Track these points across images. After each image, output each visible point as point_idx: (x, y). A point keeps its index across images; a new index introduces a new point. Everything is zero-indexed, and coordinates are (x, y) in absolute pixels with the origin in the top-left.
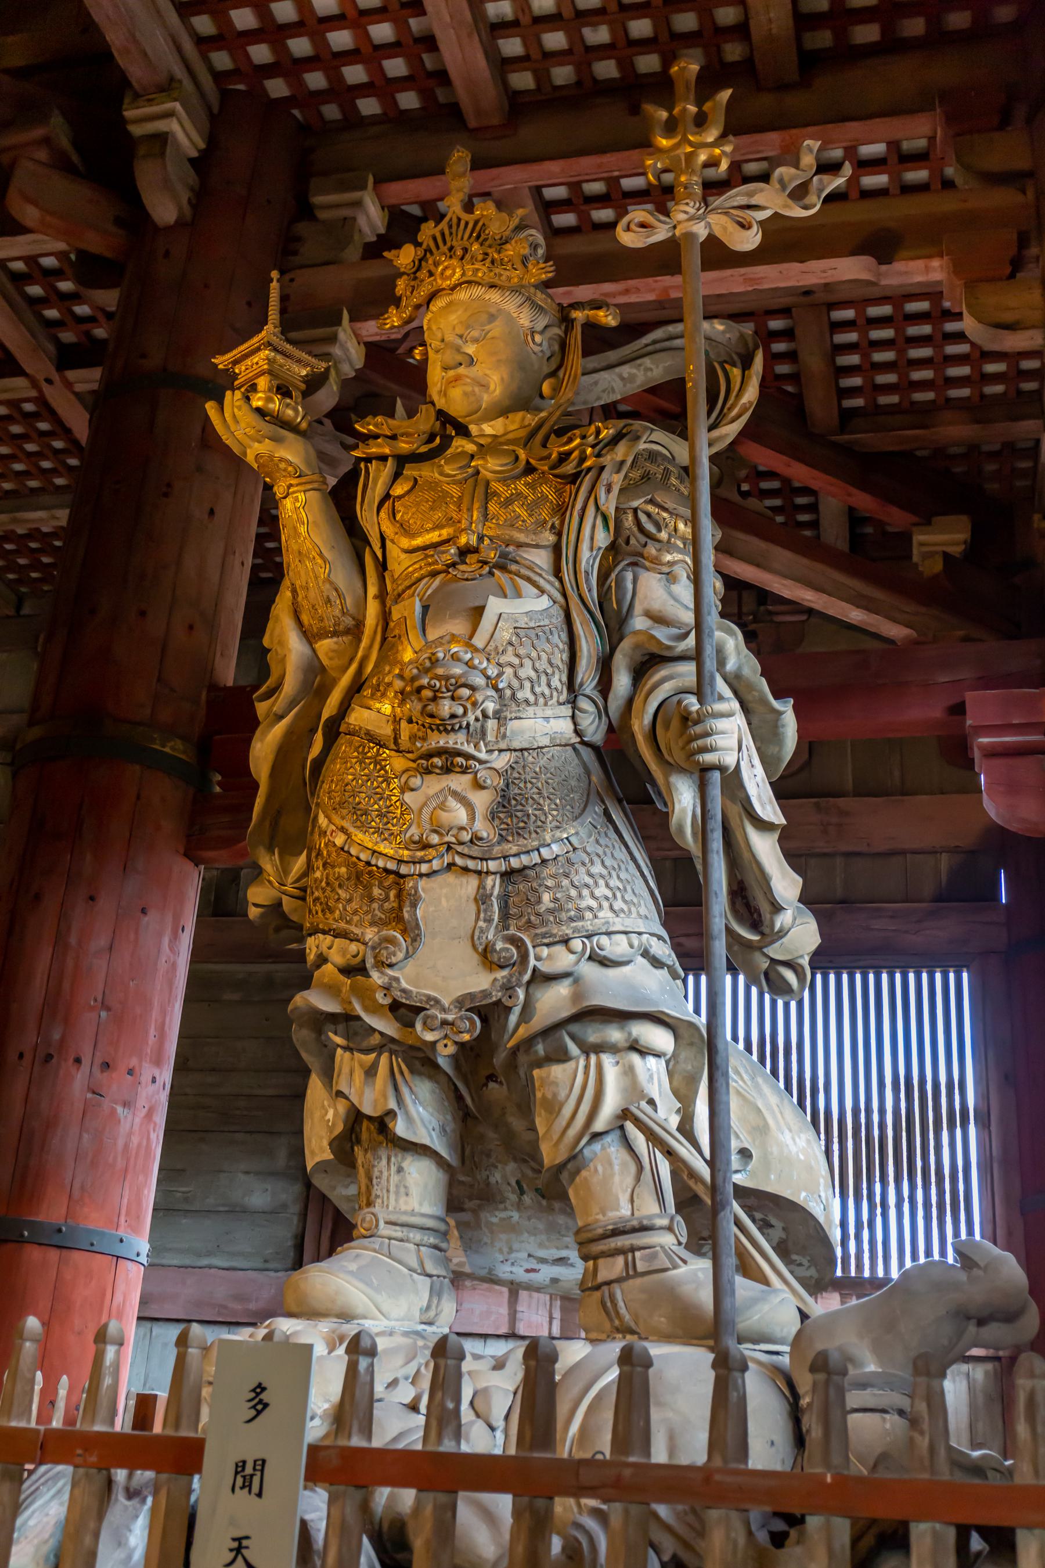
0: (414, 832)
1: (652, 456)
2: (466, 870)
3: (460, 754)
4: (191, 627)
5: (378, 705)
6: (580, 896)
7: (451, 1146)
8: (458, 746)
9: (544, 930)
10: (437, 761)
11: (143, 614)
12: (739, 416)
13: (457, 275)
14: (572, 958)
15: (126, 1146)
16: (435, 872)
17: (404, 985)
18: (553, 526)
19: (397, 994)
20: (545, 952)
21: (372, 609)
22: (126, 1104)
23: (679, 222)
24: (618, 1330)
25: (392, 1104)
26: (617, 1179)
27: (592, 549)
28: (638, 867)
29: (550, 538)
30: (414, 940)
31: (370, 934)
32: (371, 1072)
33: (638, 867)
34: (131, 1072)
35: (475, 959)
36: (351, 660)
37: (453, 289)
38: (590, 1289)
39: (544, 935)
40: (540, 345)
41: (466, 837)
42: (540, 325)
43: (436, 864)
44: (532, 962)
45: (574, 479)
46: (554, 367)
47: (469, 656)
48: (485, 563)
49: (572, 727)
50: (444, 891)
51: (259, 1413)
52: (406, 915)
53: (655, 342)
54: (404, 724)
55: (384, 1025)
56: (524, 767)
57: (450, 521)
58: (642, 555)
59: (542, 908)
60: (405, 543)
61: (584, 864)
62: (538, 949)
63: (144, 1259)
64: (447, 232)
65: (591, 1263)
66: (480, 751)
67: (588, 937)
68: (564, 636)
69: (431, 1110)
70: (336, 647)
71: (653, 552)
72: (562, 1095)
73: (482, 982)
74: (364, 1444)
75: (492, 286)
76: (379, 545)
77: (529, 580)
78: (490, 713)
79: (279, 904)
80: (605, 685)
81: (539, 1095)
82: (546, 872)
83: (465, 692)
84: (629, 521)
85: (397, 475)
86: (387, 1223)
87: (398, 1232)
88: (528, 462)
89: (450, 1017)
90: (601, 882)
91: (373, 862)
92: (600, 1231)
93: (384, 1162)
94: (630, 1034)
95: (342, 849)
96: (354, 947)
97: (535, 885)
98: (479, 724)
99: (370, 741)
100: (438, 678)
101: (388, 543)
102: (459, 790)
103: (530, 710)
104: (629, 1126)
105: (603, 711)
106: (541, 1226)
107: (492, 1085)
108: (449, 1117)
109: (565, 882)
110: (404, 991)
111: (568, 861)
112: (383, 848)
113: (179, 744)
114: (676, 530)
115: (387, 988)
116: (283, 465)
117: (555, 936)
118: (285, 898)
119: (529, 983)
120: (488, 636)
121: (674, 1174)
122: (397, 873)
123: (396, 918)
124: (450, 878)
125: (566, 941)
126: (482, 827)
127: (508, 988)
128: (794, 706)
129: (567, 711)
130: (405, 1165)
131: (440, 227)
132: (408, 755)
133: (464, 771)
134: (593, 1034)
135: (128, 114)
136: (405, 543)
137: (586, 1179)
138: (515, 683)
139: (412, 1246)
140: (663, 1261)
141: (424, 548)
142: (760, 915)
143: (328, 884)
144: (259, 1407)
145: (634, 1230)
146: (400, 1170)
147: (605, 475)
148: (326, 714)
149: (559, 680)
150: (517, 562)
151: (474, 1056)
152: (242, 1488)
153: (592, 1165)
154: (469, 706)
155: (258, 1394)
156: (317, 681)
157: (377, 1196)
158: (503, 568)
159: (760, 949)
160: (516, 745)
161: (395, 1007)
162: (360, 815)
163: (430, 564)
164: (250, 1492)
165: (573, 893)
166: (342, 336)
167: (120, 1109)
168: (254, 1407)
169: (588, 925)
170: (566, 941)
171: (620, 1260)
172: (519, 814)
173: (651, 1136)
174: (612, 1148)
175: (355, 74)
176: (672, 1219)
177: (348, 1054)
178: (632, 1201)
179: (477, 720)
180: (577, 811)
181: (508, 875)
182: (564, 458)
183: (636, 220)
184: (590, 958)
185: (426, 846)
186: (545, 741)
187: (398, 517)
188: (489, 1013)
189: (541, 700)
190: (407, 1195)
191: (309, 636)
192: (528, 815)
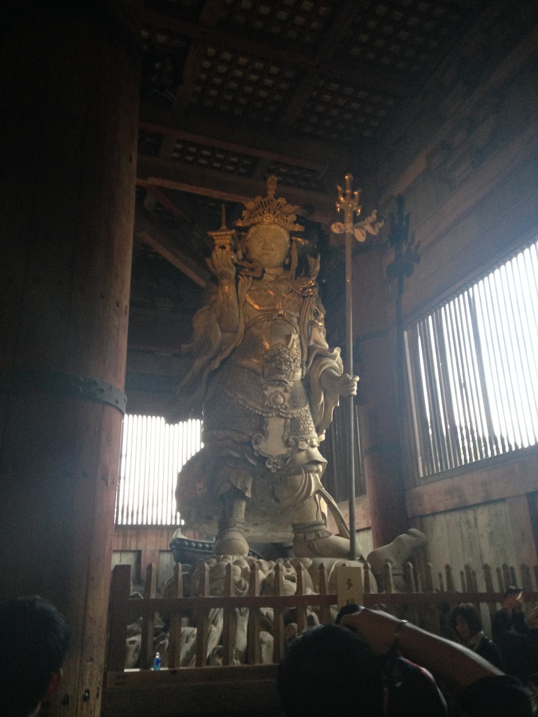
2: (282, 417)
10: (277, 383)
19: (261, 453)
41: (284, 407)
45: (304, 298)
48: (285, 320)
51: (350, 587)
52: (264, 429)
54: (266, 370)
65: (302, 535)
72: (299, 484)
73: (284, 451)
75: (282, 227)
83: (289, 363)
89: (276, 461)
96: (245, 437)
109: (306, 423)
110: (262, 452)
115: (258, 452)
122: (261, 416)
124: (277, 419)
127: (292, 453)
131: (264, 200)
133: (283, 386)
134: (309, 467)
140: (326, 534)
146: (241, 506)
158: (289, 323)
160: (295, 380)
170: (306, 441)
181: (291, 419)
185: (271, 408)
191: (223, 331)
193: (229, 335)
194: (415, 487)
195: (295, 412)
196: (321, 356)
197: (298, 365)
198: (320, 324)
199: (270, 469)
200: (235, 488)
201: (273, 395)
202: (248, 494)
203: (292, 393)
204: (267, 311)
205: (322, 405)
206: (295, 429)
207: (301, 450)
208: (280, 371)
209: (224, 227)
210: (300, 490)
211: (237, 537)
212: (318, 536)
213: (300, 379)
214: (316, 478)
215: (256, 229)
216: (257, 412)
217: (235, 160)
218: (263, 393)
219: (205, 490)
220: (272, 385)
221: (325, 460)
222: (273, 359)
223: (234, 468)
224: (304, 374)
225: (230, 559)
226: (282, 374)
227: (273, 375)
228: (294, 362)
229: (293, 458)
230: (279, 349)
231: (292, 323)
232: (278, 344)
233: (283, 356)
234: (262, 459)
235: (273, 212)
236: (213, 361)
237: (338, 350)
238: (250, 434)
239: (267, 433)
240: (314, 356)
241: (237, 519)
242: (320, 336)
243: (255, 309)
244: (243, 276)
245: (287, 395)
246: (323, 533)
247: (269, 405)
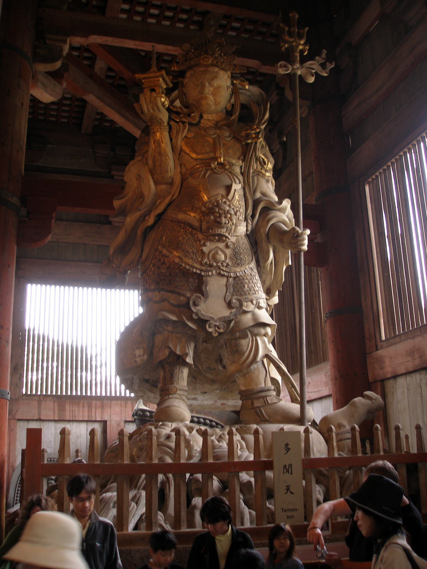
0: (206, 260)
2: (223, 276)
4: (18, 151)
13: (210, 62)
14: (253, 306)
17: (203, 313)
19: (200, 315)
24: (262, 421)
35: (225, 304)
41: (225, 265)
48: (226, 169)
51: (288, 451)
52: (203, 289)
71: (264, 172)
72: (245, 349)
73: (226, 313)
76: (179, 153)
80: (253, 216)
83: (229, 216)
89: (218, 324)
92: (255, 391)
96: (182, 298)
109: (251, 281)
110: (202, 314)
117: (248, 299)
122: (200, 275)
125: (252, 302)
127: (235, 315)
132: (205, 234)
133: (223, 241)
134: (256, 330)
143: (170, 275)
146: (182, 372)
158: (230, 172)
160: (238, 234)
170: (252, 302)
181: (234, 278)
185: (211, 266)
191: (156, 183)
193: (163, 187)
194: (377, 350)
195: (238, 269)
196: (269, 208)
197: (241, 218)
198: (267, 174)
199: (211, 332)
200: (176, 354)
201: (213, 252)
202: (189, 360)
203: (234, 250)
204: (206, 159)
205: (271, 263)
206: (238, 288)
207: (245, 312)
208: (219, 224)
209: (154, 68)
210: (246, 354)
211: (176, 404)
212: (266, 403)
213: (243, 234)
214: (264, 342)
215: (193, 72)
216: (194, 270)
217: (184, 17)
218: (201, 250)
219: (145, 357)
220: (212, 241)
221: (273, 322)
222: (211, 211)
223: (172, 332)
224: (250, 228)
225: (168, 426)
226: (222, 227)
227: (212, 230)
228: (236, 214)
229: (237, 320)
230: (218, 201)
231: (233, 172)
232: (217, 195)
233: (222, 208)
234: (202, 322)
236: (147, 218)
237: (288, 202)
238: (188, 295)
239: (207, 293)
240: (260, 210)
241: (177, 386)
242: (268, 187)
243: (192, 158)
244: (177, 122)
245: (228, 252)
247: (208, 263)
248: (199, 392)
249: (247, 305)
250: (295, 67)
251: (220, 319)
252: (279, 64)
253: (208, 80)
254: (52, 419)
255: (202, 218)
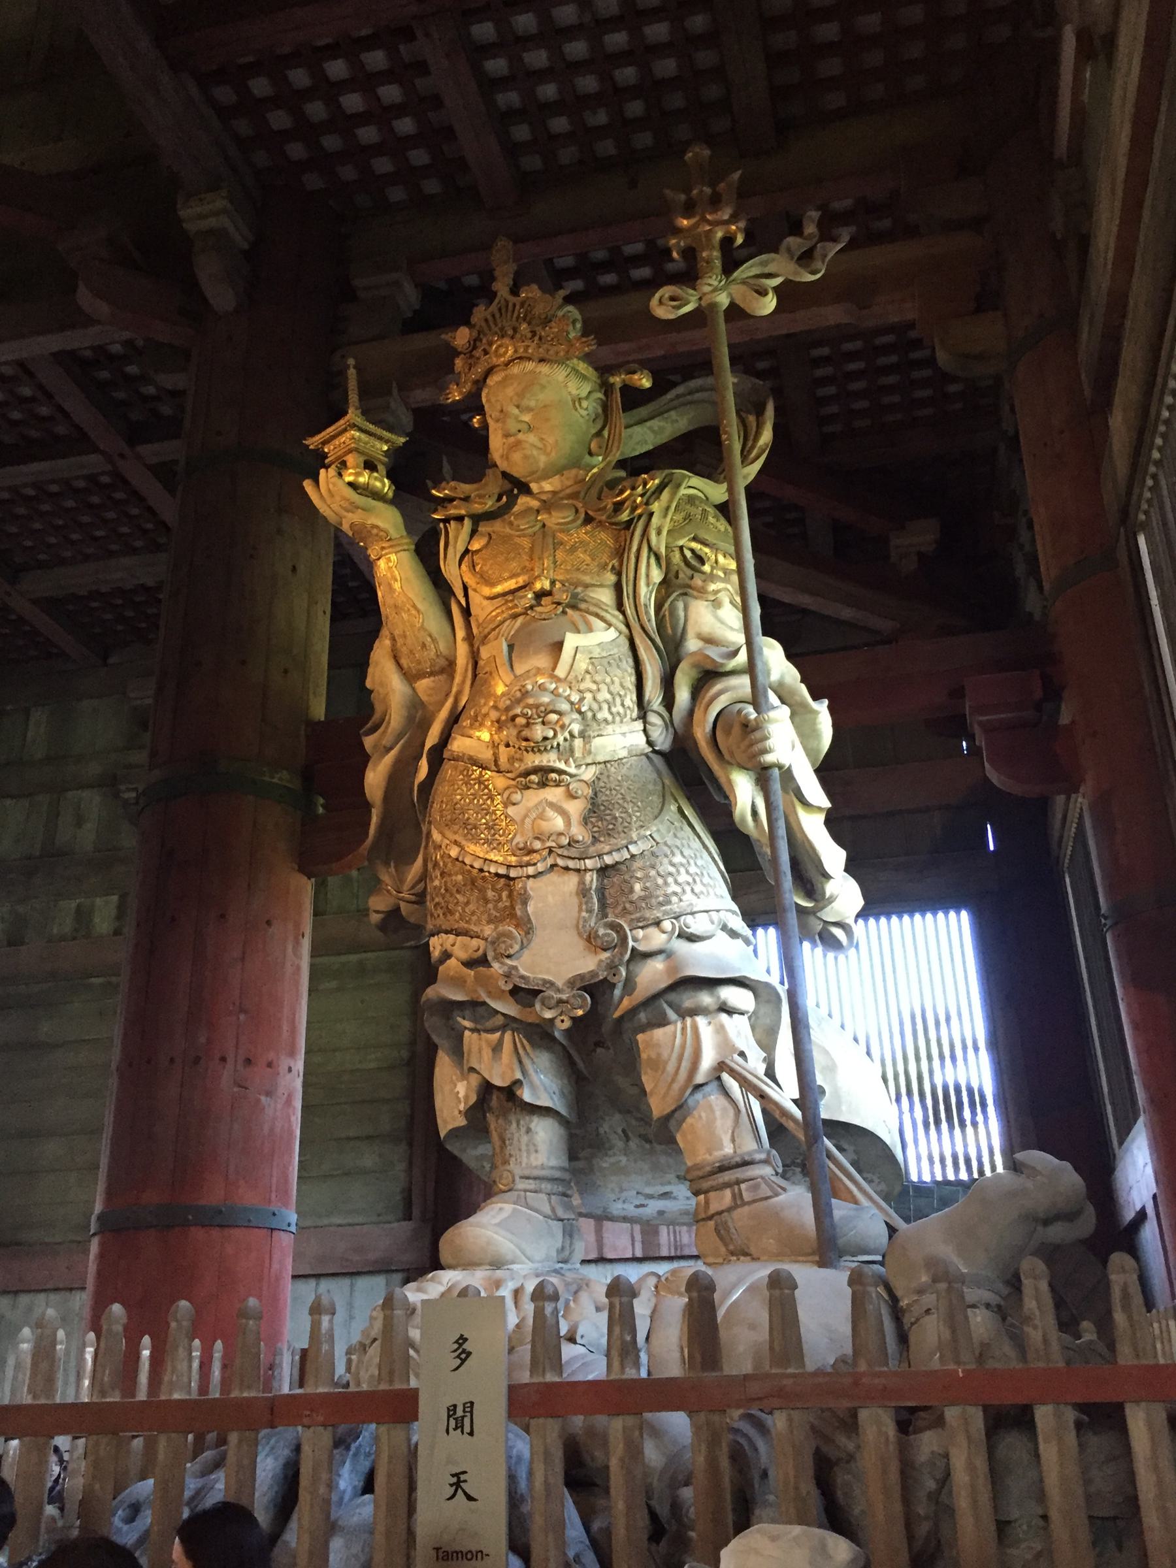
1: (691, 500)
2: (567, 869)
3: (554, 770)
4: (286, 671)
5: (478, 734)
6: (666, 883)
7: (570, 1107)
8: (551, 764)
9: (638, 915)
10: (534, 778)
11: (244, 662)
12: (757, 458)
14: (664, 936)
15: (272, 1130)
16: (541, 873)
17: (523, 972)
18: (613, 568)
20: (640, 933)
21: (462, 650)
22: (268, 1094)
23: (705, 294)
24: (732, 1254)
25: (519, 1075)
26: (719, 1123)
27: (648, 585)
28: (710, 854)
29: (611, 578)
30: (527, 933)
31: (488, 930)
32: (497, 1048)
33: (710, 854)
34: (270, 1065)
35: (582, 944)
36: (447, 695)
37: (507, 364)
38: (703, 1220)
39: (638, 920)
40: (586, 409)
41: (565, 841)
42: (584, 394)
43: (541, 867)
44: (631, 943)
46: (599, 426)
47: (554, 686)
48: (559, 604)
49: (644, 739)
50: (550, 888)
51: (463, 1361)
52: (519, 913)
53: (678, 397)
54: (502, 748)
55: (508, 1008)
56: (608, 777)
57: (524, 570)
58: (690, 587)
59: (635, 897)
60: (487, 591)
61: (666, 856)
62: (634, 932)
63: (293, 1229)
64: (497, 315)
65: (702, 1197)
66: (569, 766)
67: (675, 918)
68: (631, 661)
69: (550, 1075)
70: (432, 685)
72: (665, 1055)
73: (588, 964)
74: (557, 1379)
77: (597, 616)
78: (576, 734)
79: (397, 909)
80: (669, 701)
81: (644, 1056)
82: (637, 864)
84: (676, 558)
85: (474, 532)
86: (521, 1177)
87: (531, 1185)
88: (586, 513)
89: (564, 997)
90: (682, 870)
91: (486, 868)
92: (708, 1169)
93: (514, 1125)
94: (719, 998)
95: (457, 859)
96: (475, 943)
97: (627, 877)
98: (567, 744)
99: (473, 765)
100: (530, 706)
101: (471, 593)
102: (554, 801)
103: (610, 728)
104: (725, 1077)
105: (669, 724)
106: (646, 1167)
107: (599, 1050)
108: (566, 1081)
109: (653, 873)
110: (522, 977)
111: (653, 854)
112: (492, 856)
113: (285, 774)
114: (716, 562)
115: (507, 976)
116: (375, 531)
117: (647, 919)
118: (403, 905)
119: (629, 961)
120: (567, 667)
121: (765, 1112)
122: (507, 877)
123: (510, 914)
124: (553, 877)
125: (657, 923)
126: (578, 832)
127: (612, 967)
128: (830, 708)
129: (639, 725)
130: (532, 1126)
131: (491, 309)
132: (509, 775)
133: (558, 784)
134: (688, 1002)
135: (182, 213)
136: (487, 591)
137: (692, 1125)
138: (595, 706)
139: (544, 1197)
140: (765, 1191)
141: (504, 594)
142: (813, 885)
143: (446, 890)
144: (463, 1356)
145: (739, 1165)
146: (529, 1130)
147: (655, 520)
148: (429, 743)
149: (631, 699)
150: (585, 601)
151: (588, 1031)
152: (454, 1430)
153: (695, 1113)
154: (558, 729)
155: (461, 1345)
156: (419, 716)
157: (511, 1155)
158: (574, 607)
159: (814, 913)
160: (600, 759)
161: (516, 992)
162: (470, 830)
163: (511, 608)
164: (462, 1432)
165: (660, 881)
166: (393, 405)
167: (263, 1098)
168: (458, 1357)
169: (675, 907)
170: (657, 923)
171: (728, 1193)
172: (608, 818)
173: (745, 1084)
174: (715, 1099)
175: (383, 165)
176: (769, 1153)
177: (475, 1035)
178: (733, 1140)
179: (565, 740)
180: (656, 811)
181: (603, 871)
182: (618, 507)
183: (667, 296)
184: (679, 936)
186: (623, 753)
187: (478, 568)
188: (596, 989)
189: (618, 719)
190: (536, 1151)
191: (410, 677)
192: (616, 818)
205: (755, 813)
206: (615, 895)
210: (671, 1068)
212: (738, 1201)
227: (521, 760)
234: (525, 994)
235: (510, 332)
239: (529, 919)
241: (518, 1172)
246: (756, 1188)
248: (671, 1176)
249: (645, 937)
250: (707, 289)
251: (571, 983)
252: (657, 296)
253: (511, 399)
254: (629, 1255)
255: (496, 737)
